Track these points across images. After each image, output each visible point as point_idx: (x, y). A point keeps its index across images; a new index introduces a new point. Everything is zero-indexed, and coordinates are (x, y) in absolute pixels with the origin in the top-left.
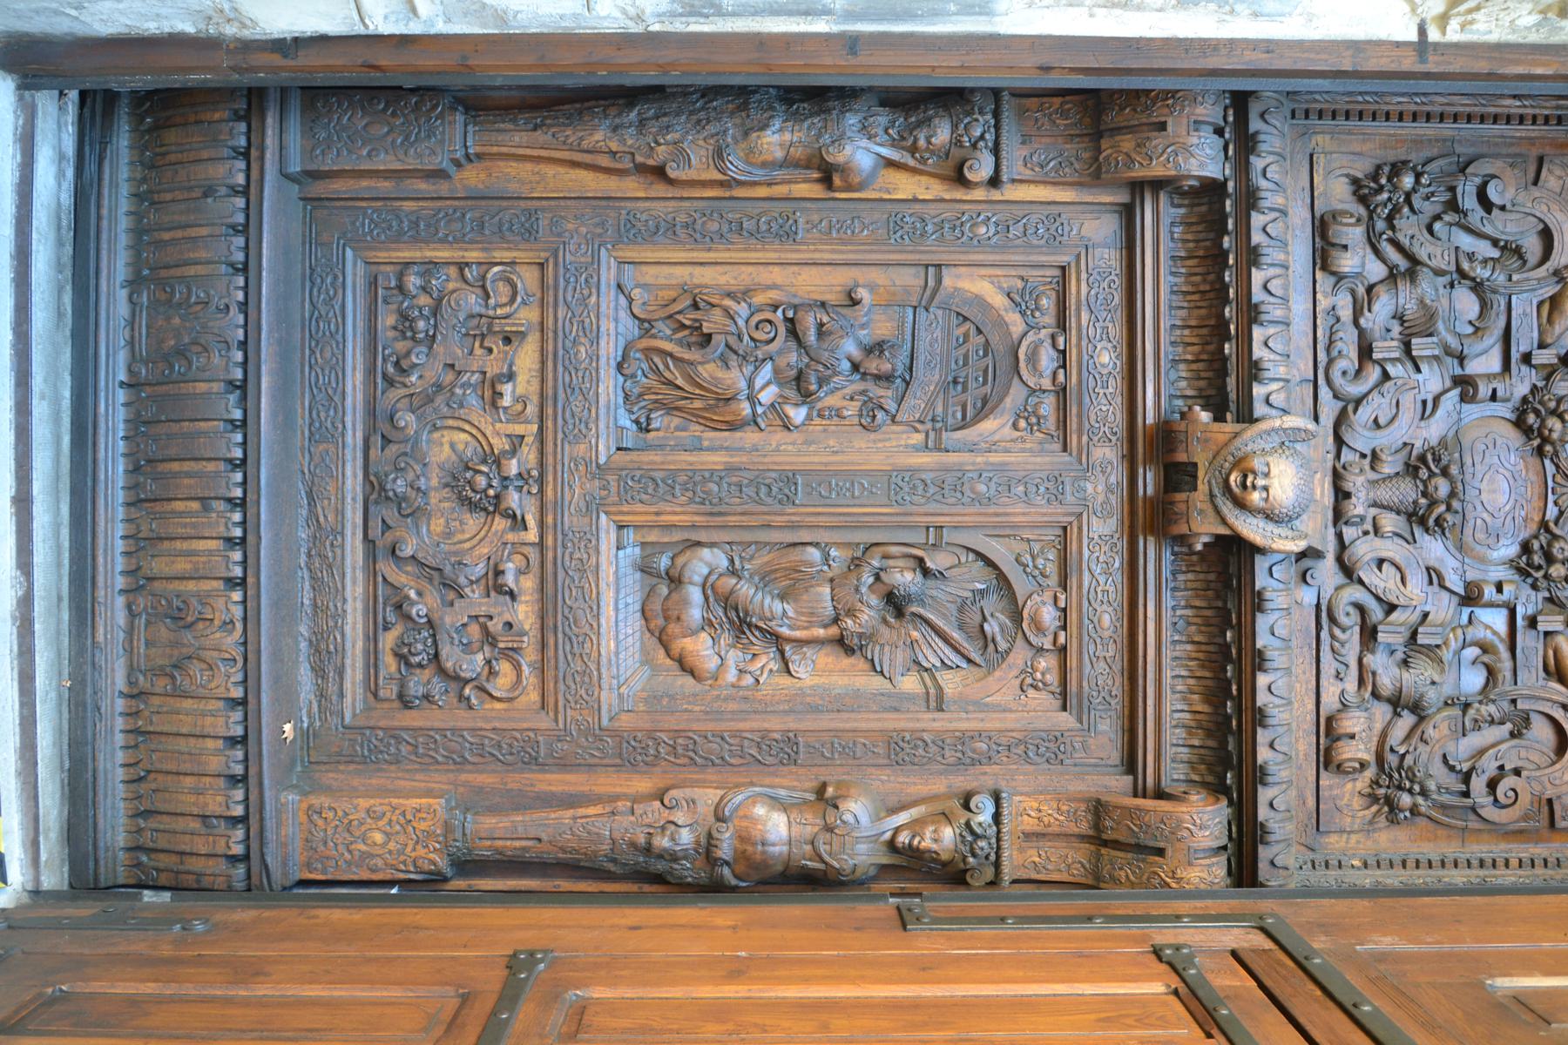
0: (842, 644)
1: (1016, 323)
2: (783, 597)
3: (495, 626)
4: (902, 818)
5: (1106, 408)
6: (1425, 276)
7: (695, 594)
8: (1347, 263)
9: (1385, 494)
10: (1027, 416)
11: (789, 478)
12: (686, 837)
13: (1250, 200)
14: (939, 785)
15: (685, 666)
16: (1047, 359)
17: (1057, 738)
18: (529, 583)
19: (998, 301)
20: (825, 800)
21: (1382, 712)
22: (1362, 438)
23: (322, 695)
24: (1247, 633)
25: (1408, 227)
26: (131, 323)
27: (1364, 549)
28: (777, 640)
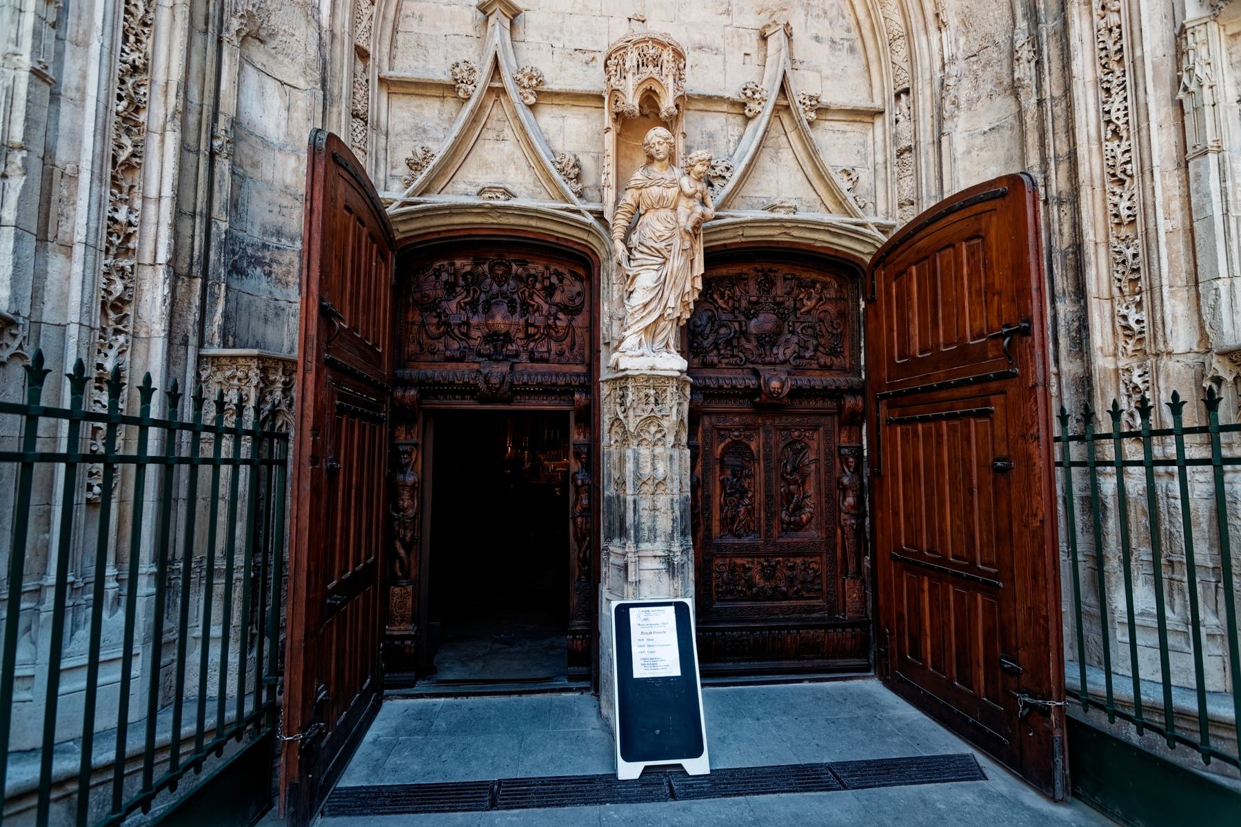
0: (804, 483)
1: (728, 440)
2: (793, 497)
3: (802, 568)
4: (846, 469)
5: (749, 420)
7: (792, 519)
8: (716, 360)
9: (768, 353)
10: (749, 438)
11: (767, 497)
12: (853, 521)
14: (838, 460)
15: (809, 521)
16: (736, 433)
17: (825, 432)
18: (791, 560)
19: (723, 445)
21: (819, 354)
23: (819, 611)
24: (806, 390)
25: (705, 343)
26: (734, 661)
27: (781, 357)
28: (803, 498)
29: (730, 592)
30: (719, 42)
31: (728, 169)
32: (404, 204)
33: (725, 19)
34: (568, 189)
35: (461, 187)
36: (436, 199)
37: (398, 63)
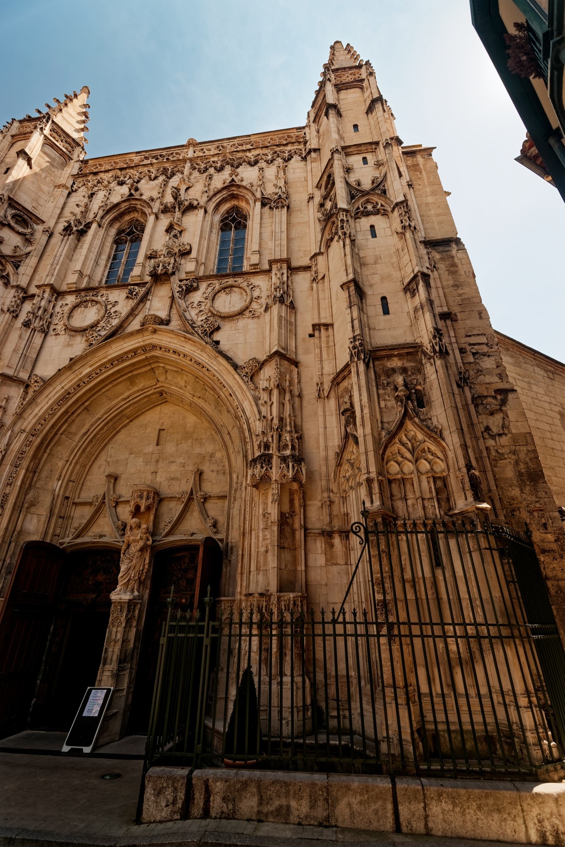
30: (179, 476)
33: (182, 469)
35: (90, 533)
36: (79, 540)
37: (82, 496)
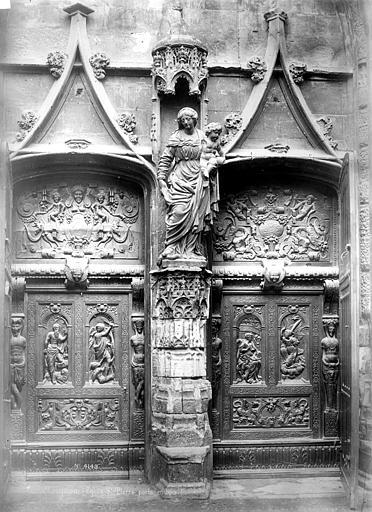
6: (235, 241)
13: (226, 276)
20: (325, 348)
22: (262, 253)
27: (282, 253)
29: (244, 421)
31: (238, 122)
32: (20, 154)
34: (127, 138)
